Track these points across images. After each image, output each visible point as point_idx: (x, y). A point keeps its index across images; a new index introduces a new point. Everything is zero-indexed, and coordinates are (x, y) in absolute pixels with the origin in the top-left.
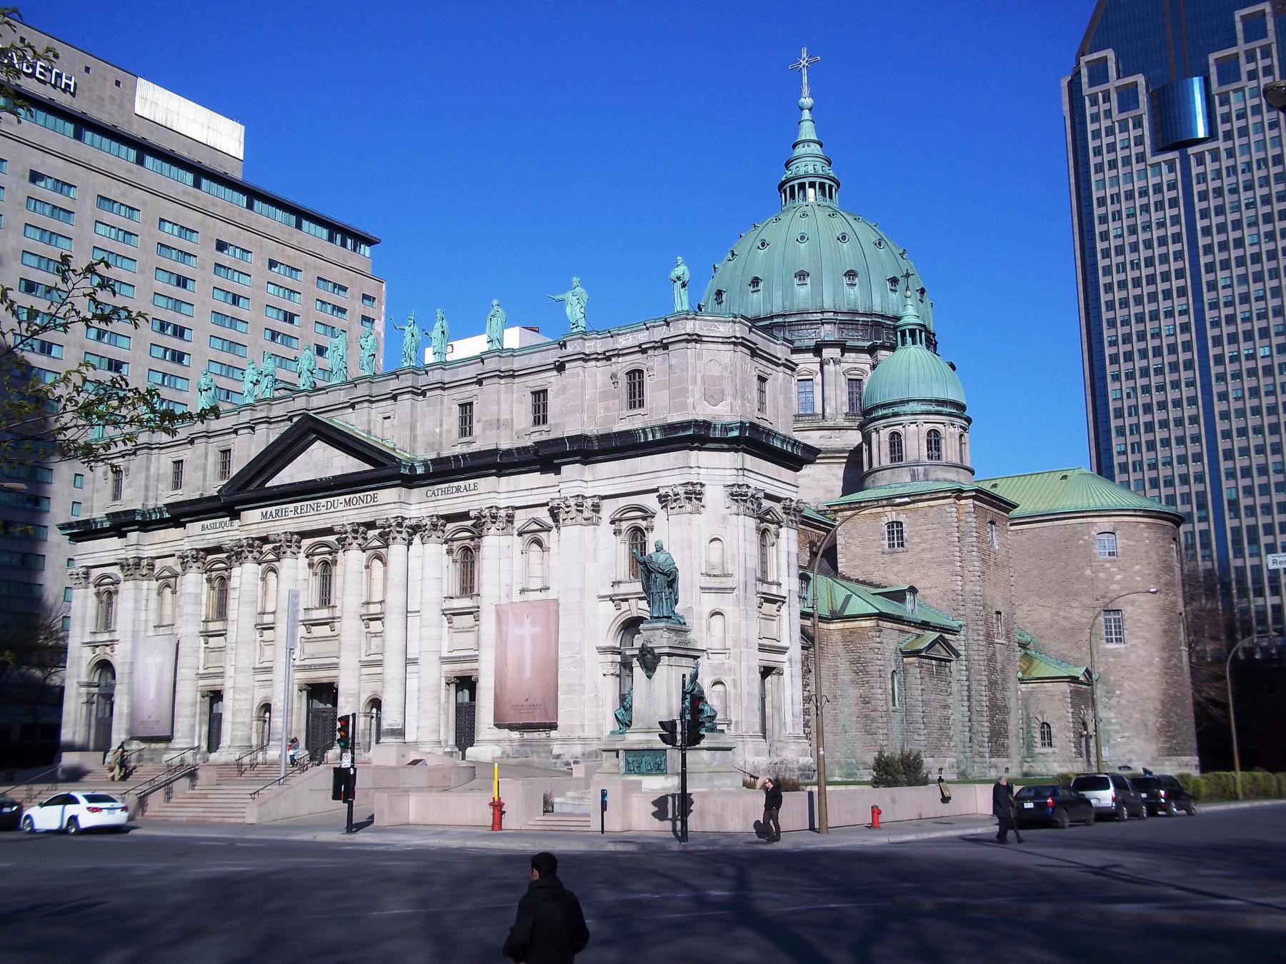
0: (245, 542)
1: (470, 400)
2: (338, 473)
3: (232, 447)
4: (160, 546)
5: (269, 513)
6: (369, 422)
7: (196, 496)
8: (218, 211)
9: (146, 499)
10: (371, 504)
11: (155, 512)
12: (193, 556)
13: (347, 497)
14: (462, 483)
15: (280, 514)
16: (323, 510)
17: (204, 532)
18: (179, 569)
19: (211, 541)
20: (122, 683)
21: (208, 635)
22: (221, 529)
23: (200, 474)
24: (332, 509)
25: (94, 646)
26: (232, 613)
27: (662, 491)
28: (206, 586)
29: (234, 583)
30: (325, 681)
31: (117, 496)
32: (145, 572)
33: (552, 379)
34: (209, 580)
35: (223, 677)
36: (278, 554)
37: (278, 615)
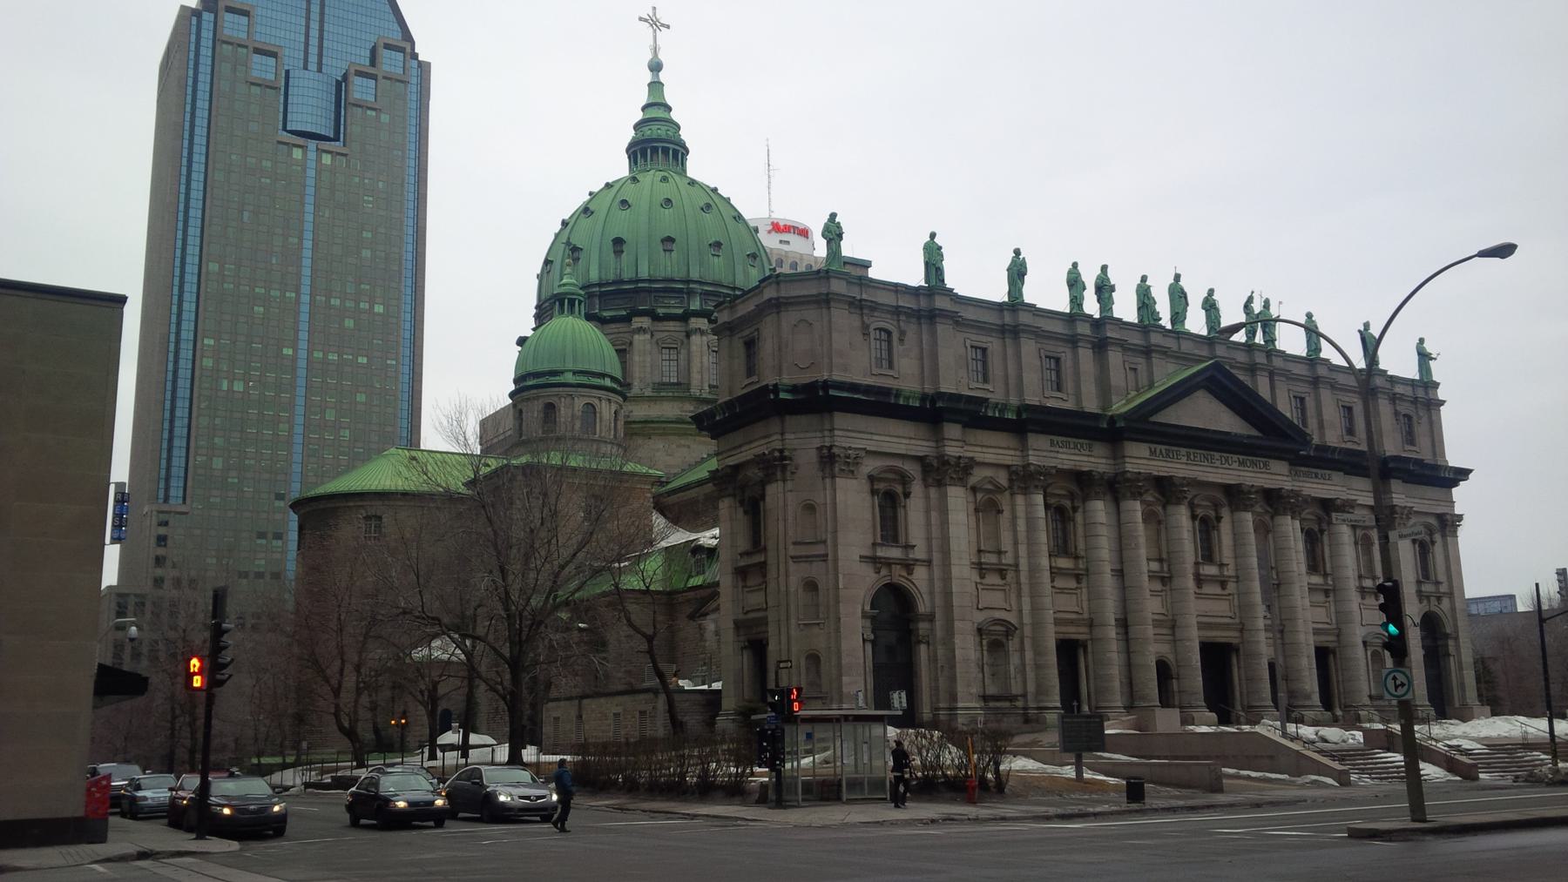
1: (1303, 395)
4: (979, 449)
5: (1158, 451)
13: (1241, 457)
14: (1319, 471)
17: (1052, 449)
19: (1065, 462)
22: (1077, 451)
27: (1448, 517)
30: (1223, 640)
33: (1356, 400)
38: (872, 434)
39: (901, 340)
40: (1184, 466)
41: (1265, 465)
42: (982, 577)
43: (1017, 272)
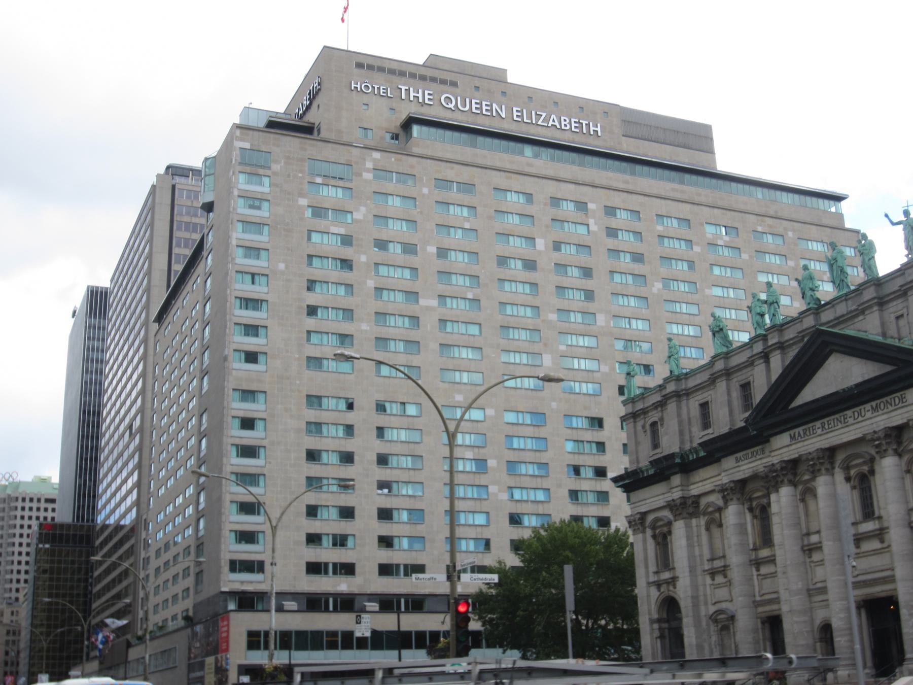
0: (778, 467)
2: (860, 380)
3: (751, 379)
4: (700, 484)
6: (883, 324)
7: (725, 430)
8: (702, 199)
9: (682, 442)
10: (901, 405)
11: (691, 453)
12: (731, 488)
13: (874, 404)
15: (808, 433)
16: (851, 421)
18: (720, 503)
19: (746, 471)
20: (687, 616)
21: (758, 563)
22: (754, 459)
23: (726, 410)
24: (860, 419)
25: (658, 585)
26: (777, 538)
28: (748, 517)
29: (774, 508)
31: (656, 445)
32: (691, 510)
34: (751, 510)
35: (779, 603)
36: (815, 473)
37: (823, 534)
38: (645, 500)
39: (662, 425)
40: (819, 439)
41: (902, 399)
42: (713, 579)
43: (718, 331)
